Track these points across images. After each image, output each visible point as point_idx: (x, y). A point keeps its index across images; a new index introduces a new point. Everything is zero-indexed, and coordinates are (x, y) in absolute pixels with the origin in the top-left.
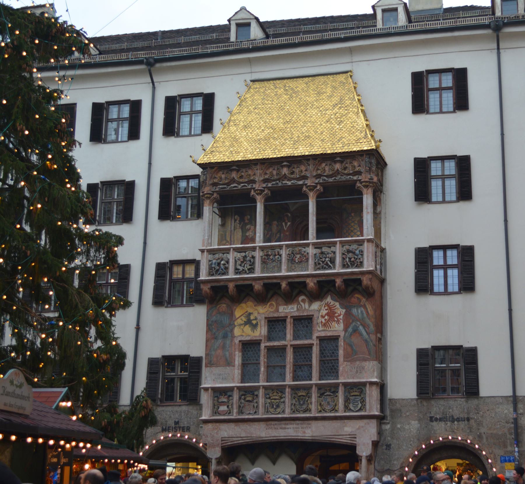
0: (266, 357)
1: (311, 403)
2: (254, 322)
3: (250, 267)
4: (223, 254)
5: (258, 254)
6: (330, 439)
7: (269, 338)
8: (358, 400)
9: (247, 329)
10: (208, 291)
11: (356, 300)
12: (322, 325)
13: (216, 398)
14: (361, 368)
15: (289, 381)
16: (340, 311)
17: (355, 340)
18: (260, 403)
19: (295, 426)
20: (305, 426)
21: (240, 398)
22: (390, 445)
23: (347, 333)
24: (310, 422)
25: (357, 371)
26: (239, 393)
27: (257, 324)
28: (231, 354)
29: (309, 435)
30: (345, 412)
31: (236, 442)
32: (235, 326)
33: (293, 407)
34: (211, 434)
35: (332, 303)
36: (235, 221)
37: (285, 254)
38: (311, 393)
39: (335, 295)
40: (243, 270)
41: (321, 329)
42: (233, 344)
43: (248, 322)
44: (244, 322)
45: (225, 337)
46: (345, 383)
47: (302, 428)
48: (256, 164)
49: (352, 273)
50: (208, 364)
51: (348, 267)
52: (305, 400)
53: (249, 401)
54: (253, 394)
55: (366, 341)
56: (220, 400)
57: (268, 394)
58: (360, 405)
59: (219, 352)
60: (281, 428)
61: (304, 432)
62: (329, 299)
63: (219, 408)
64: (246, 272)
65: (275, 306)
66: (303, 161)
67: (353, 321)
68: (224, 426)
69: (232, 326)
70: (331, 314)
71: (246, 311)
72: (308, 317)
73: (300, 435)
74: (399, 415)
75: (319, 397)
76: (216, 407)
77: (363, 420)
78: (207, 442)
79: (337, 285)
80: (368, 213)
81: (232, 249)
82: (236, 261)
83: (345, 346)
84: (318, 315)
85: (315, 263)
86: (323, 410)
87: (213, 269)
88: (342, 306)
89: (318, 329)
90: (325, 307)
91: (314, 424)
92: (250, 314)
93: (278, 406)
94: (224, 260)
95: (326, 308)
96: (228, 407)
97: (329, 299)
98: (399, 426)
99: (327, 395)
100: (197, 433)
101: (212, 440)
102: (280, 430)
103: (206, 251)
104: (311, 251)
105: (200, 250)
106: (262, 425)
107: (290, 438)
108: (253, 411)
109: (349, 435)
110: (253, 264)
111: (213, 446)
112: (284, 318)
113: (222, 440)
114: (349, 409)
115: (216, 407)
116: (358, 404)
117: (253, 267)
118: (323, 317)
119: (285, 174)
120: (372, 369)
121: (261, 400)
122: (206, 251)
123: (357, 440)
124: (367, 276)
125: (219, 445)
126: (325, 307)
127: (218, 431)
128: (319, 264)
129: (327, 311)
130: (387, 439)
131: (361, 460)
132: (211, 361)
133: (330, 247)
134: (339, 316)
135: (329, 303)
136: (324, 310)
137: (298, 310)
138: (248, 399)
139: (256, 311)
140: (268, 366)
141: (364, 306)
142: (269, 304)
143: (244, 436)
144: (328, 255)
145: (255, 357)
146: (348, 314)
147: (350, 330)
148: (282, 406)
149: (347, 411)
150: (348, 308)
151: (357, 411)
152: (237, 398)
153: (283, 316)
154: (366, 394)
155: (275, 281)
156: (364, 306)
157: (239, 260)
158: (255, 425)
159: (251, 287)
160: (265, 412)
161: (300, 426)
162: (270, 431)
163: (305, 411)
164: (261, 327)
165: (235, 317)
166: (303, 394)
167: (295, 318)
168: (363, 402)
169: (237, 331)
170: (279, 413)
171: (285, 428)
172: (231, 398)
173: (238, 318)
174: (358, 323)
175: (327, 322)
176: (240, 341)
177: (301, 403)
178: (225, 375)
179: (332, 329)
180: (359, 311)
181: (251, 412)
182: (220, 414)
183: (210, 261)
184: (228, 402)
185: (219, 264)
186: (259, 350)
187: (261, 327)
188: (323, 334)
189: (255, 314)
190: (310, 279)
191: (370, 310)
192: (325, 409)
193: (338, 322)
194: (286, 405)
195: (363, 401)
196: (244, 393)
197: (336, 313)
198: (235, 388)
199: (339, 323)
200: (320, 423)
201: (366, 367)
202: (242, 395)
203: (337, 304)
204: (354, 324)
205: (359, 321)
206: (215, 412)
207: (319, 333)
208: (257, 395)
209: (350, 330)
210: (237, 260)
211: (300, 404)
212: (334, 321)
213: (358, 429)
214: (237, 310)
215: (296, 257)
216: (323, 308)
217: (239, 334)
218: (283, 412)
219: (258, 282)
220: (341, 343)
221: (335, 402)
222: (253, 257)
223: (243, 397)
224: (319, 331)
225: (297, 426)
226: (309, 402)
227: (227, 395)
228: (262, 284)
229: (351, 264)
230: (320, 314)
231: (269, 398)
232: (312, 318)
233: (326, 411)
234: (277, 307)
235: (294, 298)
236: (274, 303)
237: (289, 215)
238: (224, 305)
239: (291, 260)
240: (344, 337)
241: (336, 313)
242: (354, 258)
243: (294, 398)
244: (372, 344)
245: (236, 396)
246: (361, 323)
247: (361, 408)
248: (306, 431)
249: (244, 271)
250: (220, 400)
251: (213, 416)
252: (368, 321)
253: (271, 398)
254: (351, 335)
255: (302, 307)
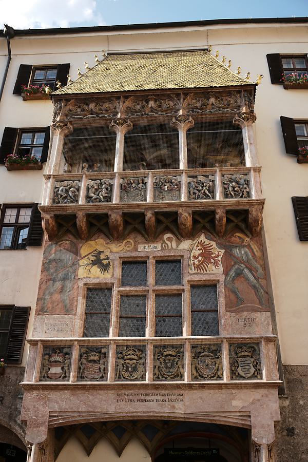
0: (119, 305)
1: (183, 366)
2: (105, 262)
3: (106, 195)
4: (73, 181)
5: (116, 183)
6: (211, 418)
7: (123, 283)
8: (249, 362)
9: (96, 270)
10: (51, 220)
11: (237, 239)
12: (195, 267)
13: (46, 357)
14: (250, 320)
15: (149, 334)
16: (218, 251)
17: (240, 285)
18: (110, 364)
19: (159, 397)
20: (174, 397)
21: (81, 357)
22: (293, 429)
23: (229, 278)
24: (182, 392)
25: (245, 324)
26: (80, 351)
27: (108, 265)
28: (72, 300)
29: (181, 411)
30: (232, 378)
31: (70, 420)
32: (80, 266)
33: (157, 371)
34: (34, 407)
35: (207, 242)
36: (83, 168)
37: (152, 181)
38: (183, 353)
39: (210, 234)
40: (97, 198)
41: (193, 272)
42: (76, 287)
43: (97, 262)
44: (91, 262)
45: (65, 279)
46: (230, 338)
47: (171, 401)
48: (119, 98)
49: (238, 203)
50: (40, 311)
51: (232, 197)
52: (174, 361)
53: (94, 362)
54: (100, 352)
55: (254, 287)
56: (52, 359)
57: (121, 353)
58: (253, 370)
59: (57, 297)
60: (138, 400)
61: (173, 407)
62: (202, 238)
63: (49, 369)
64: (100, 201)
65: (133, 244)
66: (172, 95)
67: (235, 263)
68: (54, 395)
69: (75, 264)
70: (206, 255)
71: (95, 249)
72: (176, 258)
73: (166, 410)
74: (300, 387)
75: (194, 358)
76: (46, 368)
77: (258, 390)
78: (27, 419)
79: (217, 216)
80: (251, 144)
81: (84, 176)
82: (88, 189)
83: (227, 293)
84: (189, 256)
85: (189, 191)
86: (199, 375)
87: (59, 196)
88: (220, 246)
89: (190, 271)
90: (197, 246)
91: (188, 395)
92: (100, 253)
93: (135, 369)
94: (74, 187)
95: (199, 248)
96: (62, 369)
97: (202, 238)
98: (301, 402)
99: (205, 356)
100: (13, 407)
101: (35, 416)
102: (138, 403)
103: (52, 177)
104: (184, 179)
105: (45, 175)
106: (111, 394)
107: (152, 414)
108: (98, 375)
109: (240, 412)
110: (110, 192)
111: (38, 426)
112: (145, 259)
113: (50, 416)
114: (237, 375)
115: (46, 368)
116: (250, 368)
117: (109, 195)
118: (195, 257)
119: (151, 107)
120: (266, 322)
121: (111, 360)
122: (52, 177)
123: (252, 419)
124: (256, 206)
125: (45, 422)
126: (197, 246)
127: (45, 403)
128: (194, 193)
129: (201, 251)
130: (287, 420)
131: (258, 451)
132: (44, 308)
133: (207, 177)
134: (217, 256)
135: (203, 242)
136: (197, 250)
137: (162, 249)
138: (91, 358)
139: (109, 250)
140: (120, 318)
141: (249, 246)
142: (125, 241)
143: (83, 410)
144: (205, 184)
145: (103, 306)
146: (228, 255)
147: (232, 273)
148: (141, 368)
149: (234, 377)
150: (228, 249)
151: (249, 378)
152: (77, 357)
153: (142, 255)
154: (259, 354)
155: (137, 210)
156: (249, 246)
157: (93, 187)
158: (100, 395)
159: (106, 216)
160: (116, 375)
161: (166, 398)
162: (122, 404)
163: (173, 378)
164: (113, 267)
165: (80, 256)
166: (173, 353)
167: (158, 259)
168: (256, 365)
169: (82, 272)
170: (136, 378)
171: (145, 400)
172: (67, 356)
173: (84, 257)
174: (242, 265)
175: (202, 263)
176: (85, 284)
177: (168, 365)
178: (62, 327)
179: (208, 272)
180: (243, 252)
181: (96, 377)
182: (50, 379)
183: (56, 188)
184: (64, 362)
185: (67, 192)
186: (110, 297)
187: (113, 267)
188: (196, 278)
189: (107, 253)
190: (184, 209)
191: (257, 251)
192: (203, 374)
193: (216, 264)
194: (148, 368)
195: (257, 365)
196: (87, 350)
197: (212, 254)
198: (76, 343)
199: (217, 265)
200: (197, 394)
201: (257, 319)
202: (84, 353)
203: (214, 244)
204: (237, 266)
205: (241, 263)
206: (44, 375)
207: (192, 276)
208: (105, 354)
209: (232, 273)
210: (90, 187)
211: (166, 367)
212: (211, 263)
213: (253, 403)
214: (83, 248)
215: (165, 186)
216: (195, 247)
217: (85, 275)
218: (142, 377)
219: (115, 211)
220: (221, 289)
221: (217, 365)
222: (111, 186)
223: (85, 355)
224: (190, 275)
225: (162, 398)
226: (179, 363)
227: (62, 352)
228: (121, 213)
229: (235, 194)
230: (192, 255)
231: (123, 358)
232: (179, 261)
233: (204, 378)
234: (135, 245)
235: (158, 236)
236: (131, 241)
237: (145, 164)
238: (68, 242)
239: (159, 187)
240: (224, 282)
241: (212, 254)
242: (239, 187)
243: (158, 359)
244: (262, 291)
245: (75, 354)
246: (244, 265)
247: (254, 373)
248: (176, 406)
249: (98, 200)
250: (52, 359)
251: (40, 380)
252: (256, 263)
253: (126, 357)
254: (233, 280)
255: (168, 246)
